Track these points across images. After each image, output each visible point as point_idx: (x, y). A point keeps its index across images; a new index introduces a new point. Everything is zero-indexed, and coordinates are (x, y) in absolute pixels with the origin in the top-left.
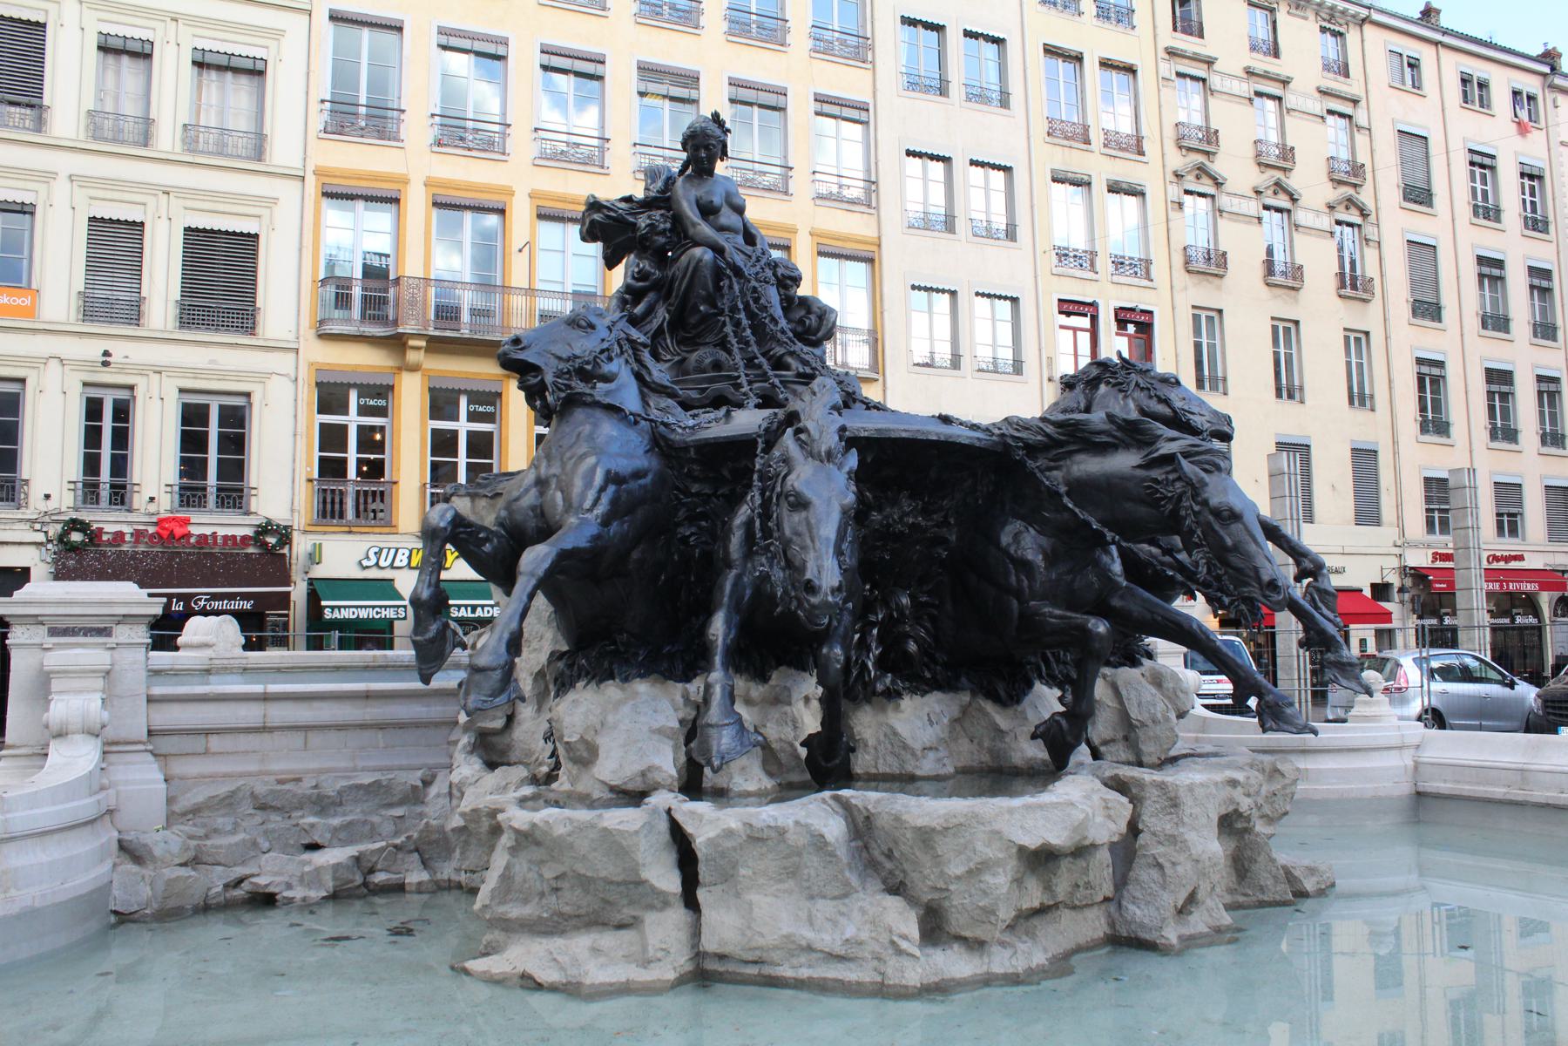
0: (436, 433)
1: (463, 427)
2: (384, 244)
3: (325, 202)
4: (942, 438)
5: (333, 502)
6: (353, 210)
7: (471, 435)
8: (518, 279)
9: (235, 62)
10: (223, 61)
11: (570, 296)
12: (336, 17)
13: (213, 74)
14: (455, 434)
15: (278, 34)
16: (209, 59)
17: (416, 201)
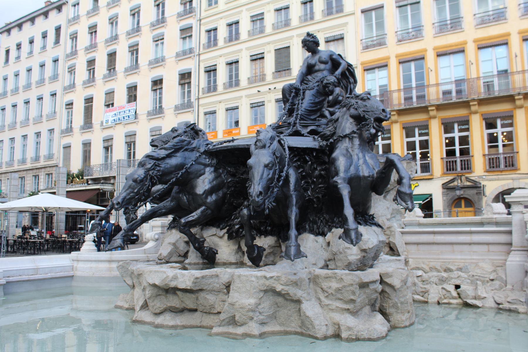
0: (408, 143)
1: (417, 139)
2: (384, 82)
3: (366, 72)
4: (232, 147)
5: (509, 161)
6: (374, 73)
7: (420, 142)
8: (433, 81)
9: (336, 38)
10: (333, 38)
11: (454, 82)
12: (363, 12)
13: (332, 43)
14: (414, 142)
15: (346, 24)
16: (329, 39)
17: (393, 63)
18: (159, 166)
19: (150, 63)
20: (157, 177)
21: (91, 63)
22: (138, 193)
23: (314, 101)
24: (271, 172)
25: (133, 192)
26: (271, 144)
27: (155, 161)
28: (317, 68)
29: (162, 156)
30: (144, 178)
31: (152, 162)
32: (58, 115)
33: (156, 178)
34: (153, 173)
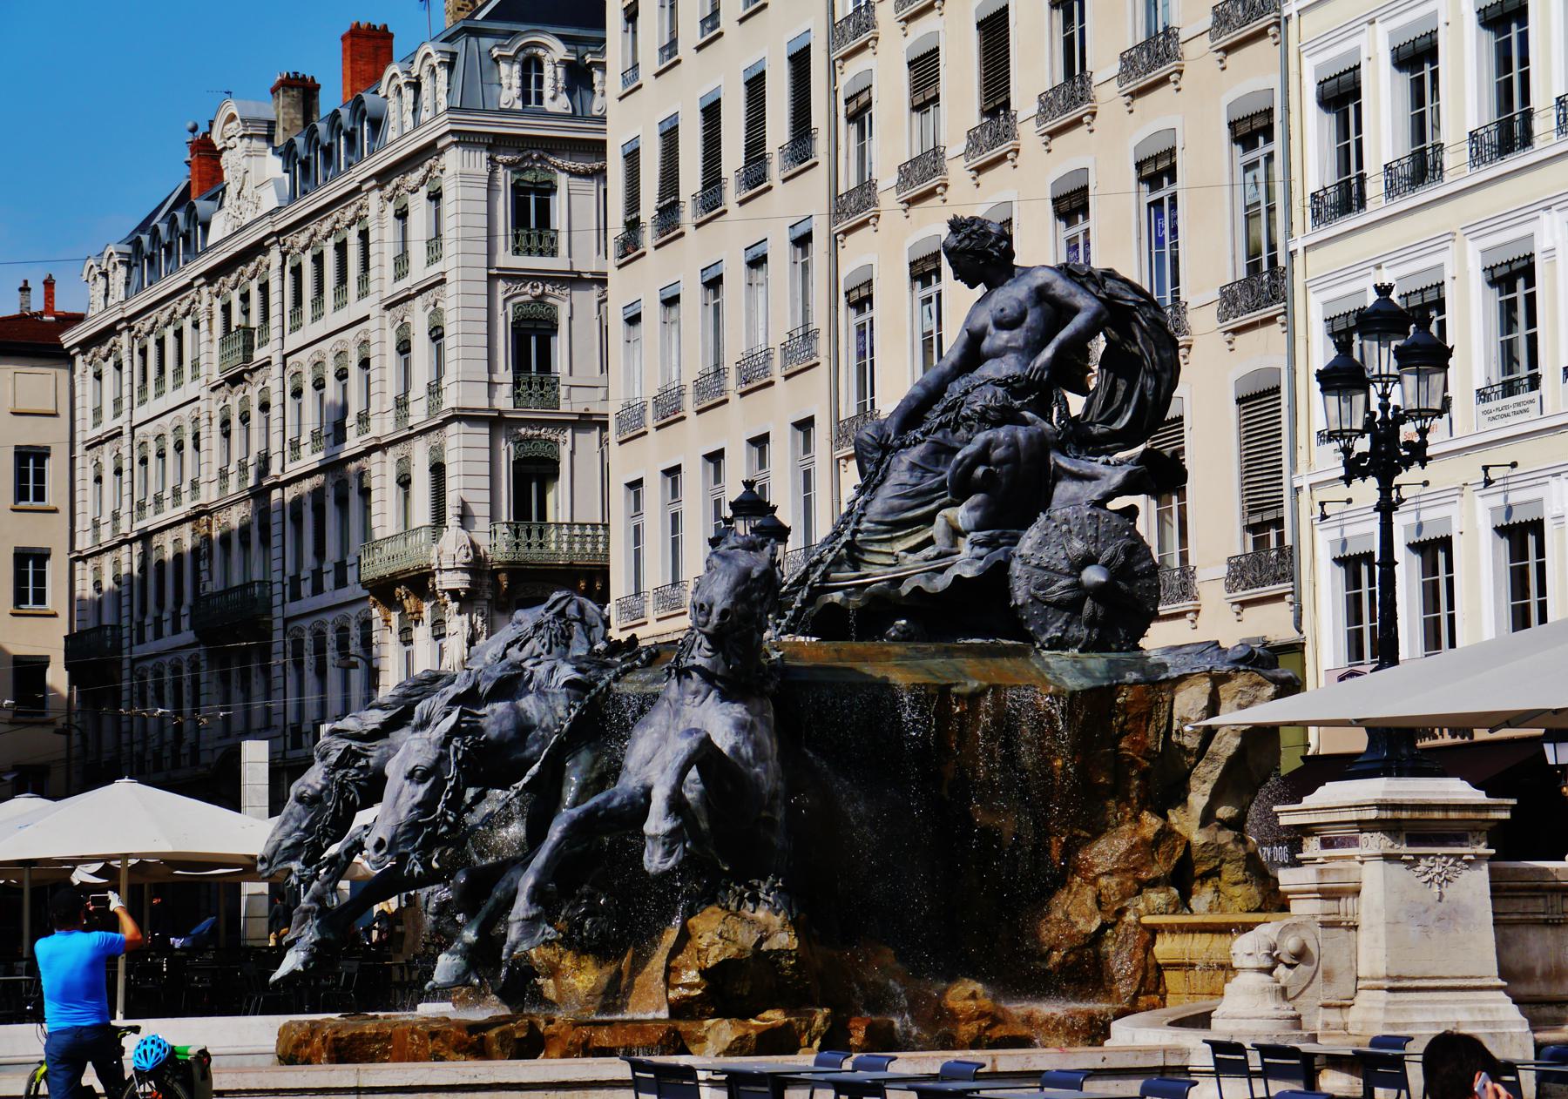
18: (366, 756)
19: (1129, 64)
20: (358, 786)
21: (925, 68)
22: (308, 830)
23: (914, 485)
24: (422, 790)
25: (297, 829)
26: (447, 714)
27: (347, 743)
28: (986, 344)
29: (370, 728)
30: (322, 791)
31: (344, 744)
32: (822, 345)
33: (352, 788)
34: (344, 776)
